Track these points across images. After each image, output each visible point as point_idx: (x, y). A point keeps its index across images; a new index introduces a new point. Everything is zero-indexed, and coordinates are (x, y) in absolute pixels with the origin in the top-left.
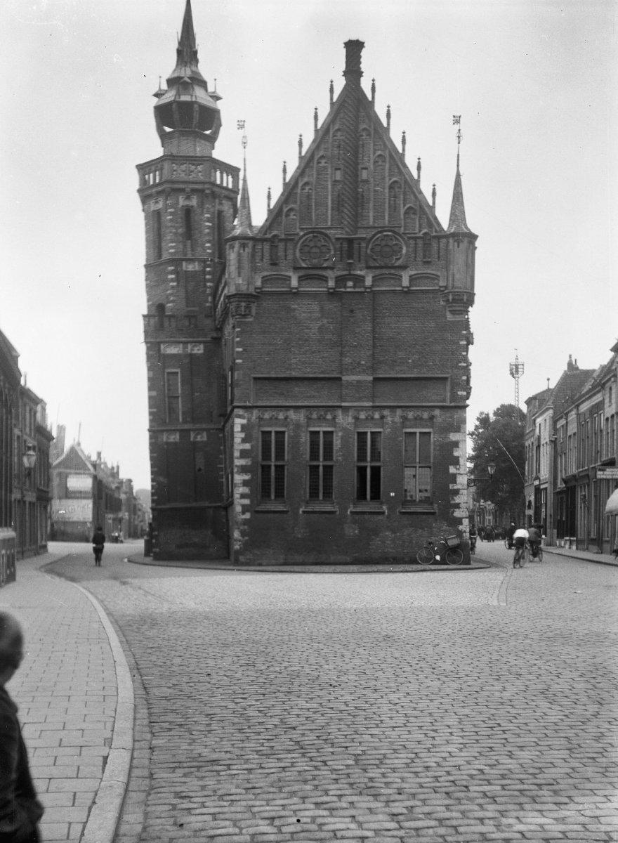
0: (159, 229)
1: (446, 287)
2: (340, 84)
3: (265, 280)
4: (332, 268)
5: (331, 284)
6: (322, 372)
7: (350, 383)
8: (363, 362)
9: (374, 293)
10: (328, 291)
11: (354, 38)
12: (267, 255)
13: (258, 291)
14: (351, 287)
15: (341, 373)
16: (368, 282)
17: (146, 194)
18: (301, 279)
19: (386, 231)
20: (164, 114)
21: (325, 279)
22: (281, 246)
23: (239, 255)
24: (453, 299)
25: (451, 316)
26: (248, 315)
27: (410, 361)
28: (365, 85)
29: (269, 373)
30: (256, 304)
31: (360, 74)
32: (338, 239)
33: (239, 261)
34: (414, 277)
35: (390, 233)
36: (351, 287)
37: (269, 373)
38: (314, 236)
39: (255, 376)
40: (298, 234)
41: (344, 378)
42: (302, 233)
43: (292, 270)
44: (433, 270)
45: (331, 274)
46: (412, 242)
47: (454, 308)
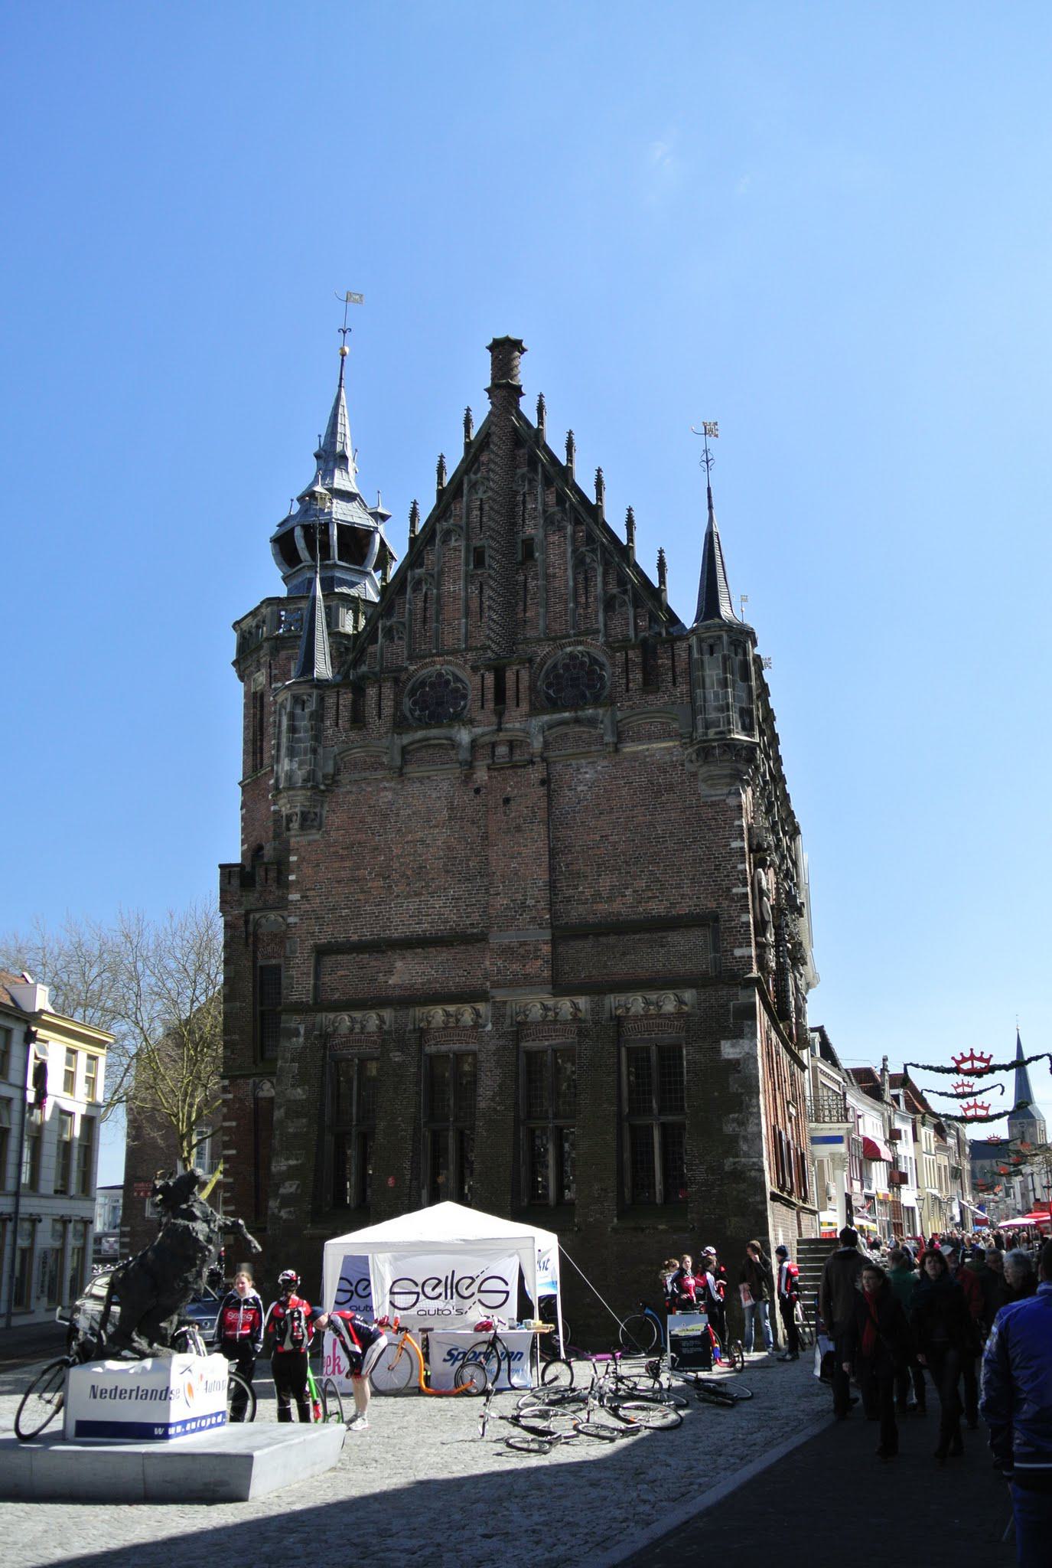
0: (262, 719)
2: (482, 410)
7: (507, 952)
11: (500, 335)
12: (345, 714)
17: (243, 664)
20: (284, 545)
21: (454, 745)
22: (372, 692)
23: (292, 717)
28: (527, 407)
31: (517, 391)
33: (293, 729)
35: (580, 648)
40: (406, 669)
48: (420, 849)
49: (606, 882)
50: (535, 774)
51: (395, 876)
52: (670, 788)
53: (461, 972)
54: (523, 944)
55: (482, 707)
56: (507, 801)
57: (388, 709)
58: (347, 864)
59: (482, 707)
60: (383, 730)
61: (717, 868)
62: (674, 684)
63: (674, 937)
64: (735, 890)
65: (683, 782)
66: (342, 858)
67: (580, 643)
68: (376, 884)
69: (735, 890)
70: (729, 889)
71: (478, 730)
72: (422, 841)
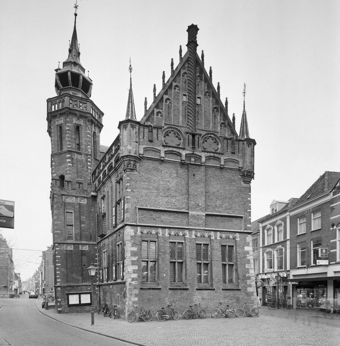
1: (242, 168)
3: (146, 150)
4: (184, 149)
5: (184, 158)
6: (177, 208)
8: (200, 205)
9: (207, 167)
10: (181, 162)
14: (193, 162)
15: (188, 210)
16: (203, 160)
18: (166, 153)
19: (210, 134)
21: (180, 155)
24: (247, 175)
25: (244, 184)
26: (134, 170)
27: (224, 206)
29: (147, 206)
30: (139, 164)
32: (187, 133)
34: (226, 160)
35: (213, 136)
36: (193, 162)
37: (147, 206)
38: (172, 131)
41: (191, 213)
42: (165, 127)
43: (161, 146)
45: (184, 153)
46: (225, 141)
47: (246, 180)
48: (168, 184)
49: (219, 203)
50: (203, 169)
51: (161, 190)
52: (235, 181)
53: (180, 221)
54: (198, 215)
55: (188, 145)
56: (194, 175)
58: (146, 183)
59: (188, 145)
61: (244, 204)
62: (239, 153)
64: (248, 210)
65: (238, 180)
66: (144, 181)
70: (247, 210)
71: (188, 152)
72: (169, 181)
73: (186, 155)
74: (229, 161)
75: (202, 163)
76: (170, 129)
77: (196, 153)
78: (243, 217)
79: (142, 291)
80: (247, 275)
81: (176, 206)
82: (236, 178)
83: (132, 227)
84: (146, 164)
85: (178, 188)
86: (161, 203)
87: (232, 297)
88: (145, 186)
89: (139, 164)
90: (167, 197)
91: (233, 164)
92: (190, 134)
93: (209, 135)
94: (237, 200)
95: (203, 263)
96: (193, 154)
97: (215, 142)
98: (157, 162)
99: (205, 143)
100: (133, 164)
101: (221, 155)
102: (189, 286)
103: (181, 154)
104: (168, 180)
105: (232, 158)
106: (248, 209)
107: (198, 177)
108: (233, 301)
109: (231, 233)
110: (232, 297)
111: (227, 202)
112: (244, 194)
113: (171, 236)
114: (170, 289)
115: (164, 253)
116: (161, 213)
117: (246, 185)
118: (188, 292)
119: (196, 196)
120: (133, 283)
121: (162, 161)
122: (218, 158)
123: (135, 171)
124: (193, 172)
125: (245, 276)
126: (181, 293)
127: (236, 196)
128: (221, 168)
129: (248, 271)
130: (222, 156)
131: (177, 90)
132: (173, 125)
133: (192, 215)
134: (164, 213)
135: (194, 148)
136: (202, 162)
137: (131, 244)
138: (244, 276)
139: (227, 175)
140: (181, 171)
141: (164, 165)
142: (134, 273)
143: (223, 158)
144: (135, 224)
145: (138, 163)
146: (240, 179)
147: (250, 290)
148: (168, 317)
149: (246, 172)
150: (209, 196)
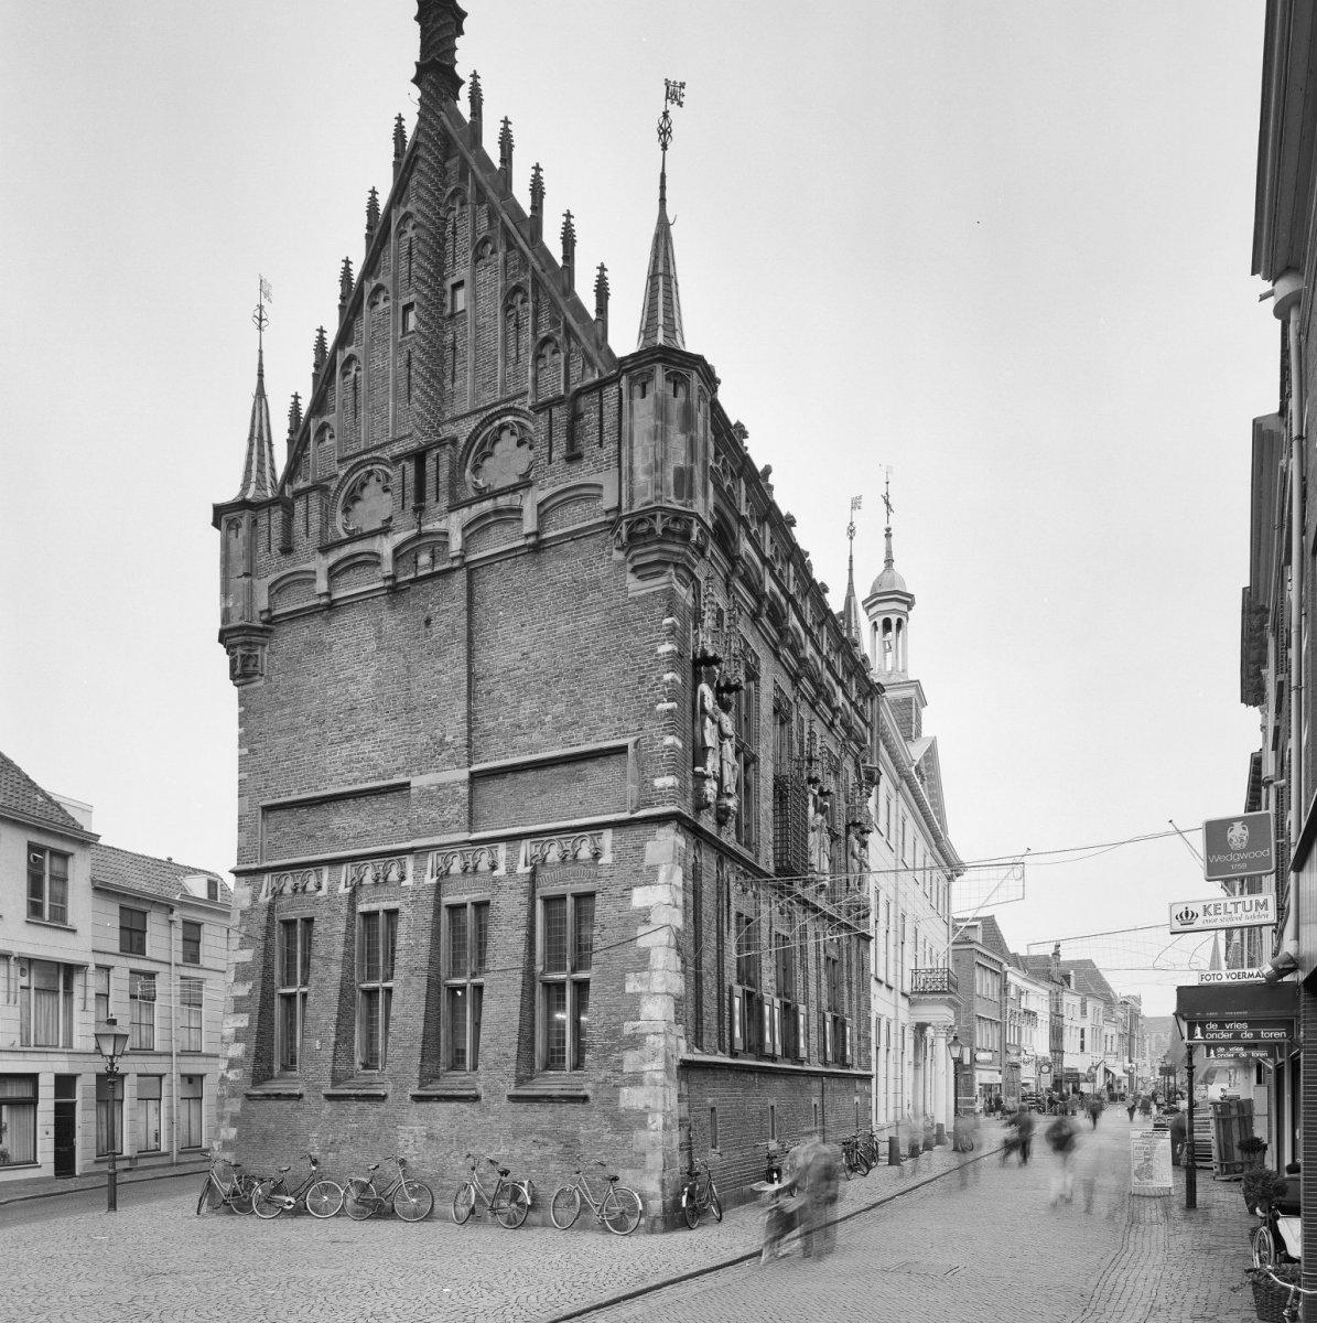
4: (384, 531)
6: (380, 777)
8: (449, 739)
9: (472, 570)
12: (276, 535)
13: (265, 617)
19: (499, 415)
25: (640, 584)
27: (548, 718)
34: (547, 506)
38: (370, 473)
39: (265, 803)
41: (418, 782)
43: (317, 554)
44: (590, 474)
45: (386, 546)
47: (639, 562)
48: (352, 688)
49: (528, 707)
52: (595, 585)
53: (389, 823)
54: (441, 787)
55: (403, 507)
56: (428, 622)
57: (315, 527)
58: (287, 711)
59: (403, 507)
60: (311, 550)
63: (591, 768)
64: (660, 707)
66: (283, 705)
67: (508, 411)
68: (313, 731)
69: (660, 707)
72: (352, 679)
73: (396, 551)
74: (564, 503)
75: (453, 559)
76: (360, 472)
77: (427, 528)
78: (626, 747)
79: (252, 1106)
80: (628, 1028)
81: (375, 767)
82: (602, 570)
83: (250, 879)
84: (290, 639)
85: (383, 694)
86: (331, 770)
87: (543, 1133)
88: (285, 723)
89: (267, 649)
90: (348, 739)
91: (576, 510)
92: (407, 456)
93: (497, 423)
94: (605, 672)
95: (469, 985)
96: (419, 536)
97: (520, 443)
98: (318, 620)
99: (488, 463)
100: (242, 656)
101: (521, 492)
102: (391, 1086)
103: (377, 555)
104: (348, 673)
105: (568, 485)
106: (659, 701)
107: (438, 629)
108: (548, 1151)
109: (578, 835)
110: (543, 1133)
111: (563, 693)
112: (637, 634)
113: (364, 889)
114: (329, 1097)
115: (327, 960)
116: (331, 807)
117: (648, 583)
118: (382, 1108)
119: (436, 707)
120: (231, 1075)
121: (331, 607)
122: (511, 510)
123: (257, 677)
124: (424, 608)
125: (620, 1031)
126: (361, 1112)
127: (604, 652)
128: (538, 547)
129: (633, 1006)
130: (528, 493)
131: (382, 306)
132: (366, 451)
133: (420, 789)
134: (340, 804)
135: (419, 510)
136: (451, 555)
137: (238, 941)
138: (614, 1033)
139: (559, 568)
140: (390, 620)
141: (338, 621)
142: (237, 1040)
143: (529, 503)
144: (254, 866)
145: (264, 645)
146: (621, 564)
147: (631, 1098)
148: (289, 1203)
149: (627, 524)
150: (489, 693)
